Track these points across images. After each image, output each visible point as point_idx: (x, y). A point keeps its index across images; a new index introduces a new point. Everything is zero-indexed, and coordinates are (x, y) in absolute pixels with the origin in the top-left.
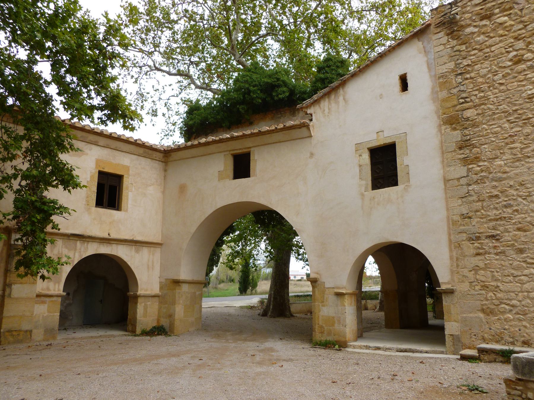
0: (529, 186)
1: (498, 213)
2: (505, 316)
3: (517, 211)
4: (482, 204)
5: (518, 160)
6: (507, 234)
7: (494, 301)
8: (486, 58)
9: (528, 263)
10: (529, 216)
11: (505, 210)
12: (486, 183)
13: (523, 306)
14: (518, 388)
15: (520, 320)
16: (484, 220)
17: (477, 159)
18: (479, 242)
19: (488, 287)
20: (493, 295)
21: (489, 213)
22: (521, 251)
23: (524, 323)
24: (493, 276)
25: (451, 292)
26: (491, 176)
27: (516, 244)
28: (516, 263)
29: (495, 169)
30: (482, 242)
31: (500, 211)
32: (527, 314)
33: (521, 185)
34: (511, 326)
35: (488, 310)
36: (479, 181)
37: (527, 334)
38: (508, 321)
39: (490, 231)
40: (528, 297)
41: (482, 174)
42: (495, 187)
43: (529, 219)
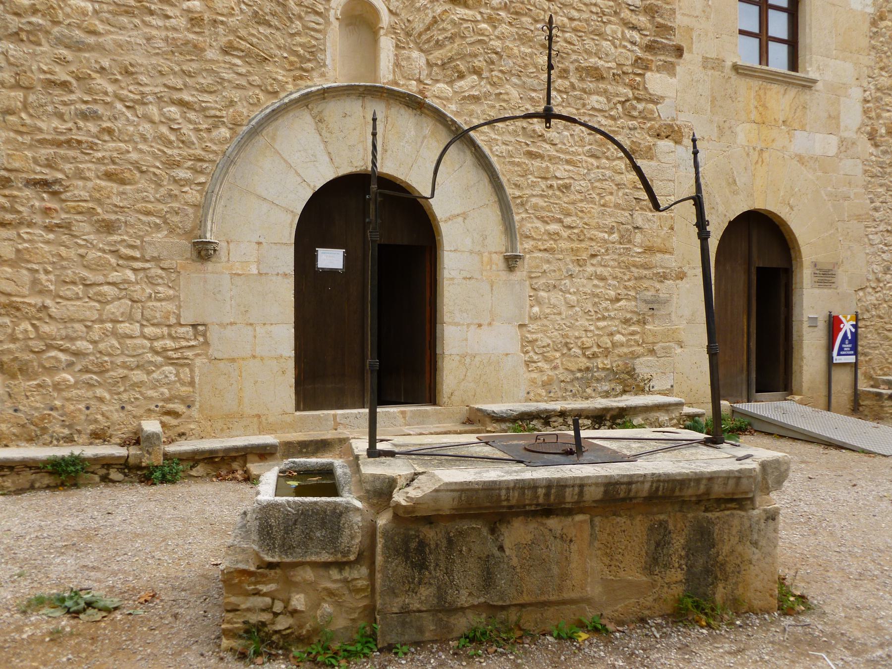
0: (144, 79)
1: (63, 127)
2: (57, 378)
3: (110, 131)
4: (25, 98)
5: (127, 12)
6: (80, 183)
7: (31, 343)
9: (121, 257)
10: (135, 149)
11: (81, 124)
12: (40, 45)
13: (100, 352)
14: (265, 589)
15: (90, 386)
16: (27, 139)
18: (7, 192)
19: (18, 309)
20: (30, 328)
21: (40, 124)
22: (108, 227)
23: (100, 392)
24: (35, 282)
26: (56, 30)
27: (99, 210)
28: (93, 254)
29: (68, 16)
30: (15, 193)
31: (70, 125)
32: (107, 371)
33: (127, 73)
34: (68, 400)
35: (16, 366)
36: (24, 36)
37: (103, 415)
38: (62, 390)
39: (38, 169)
40: (114, 333)
41: (33, 19)
42: (62, 61)
43: (134, 156)
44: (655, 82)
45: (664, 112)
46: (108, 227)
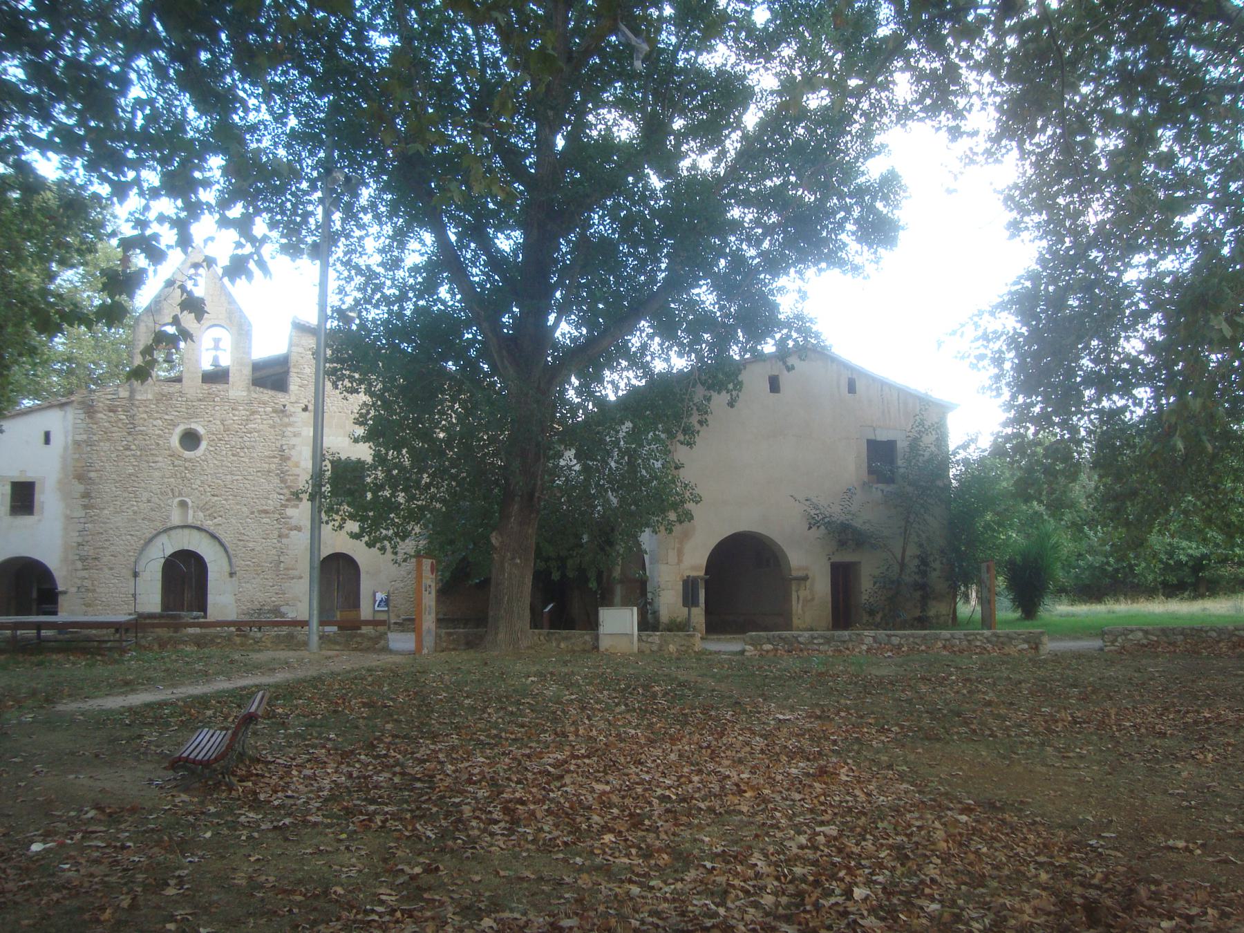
8: (109, 440)
17: (92, 507)
22: (111, 569)
25: (65, 593)
44: (290, 512)
45: (293, 522)
46: (111, 569)
